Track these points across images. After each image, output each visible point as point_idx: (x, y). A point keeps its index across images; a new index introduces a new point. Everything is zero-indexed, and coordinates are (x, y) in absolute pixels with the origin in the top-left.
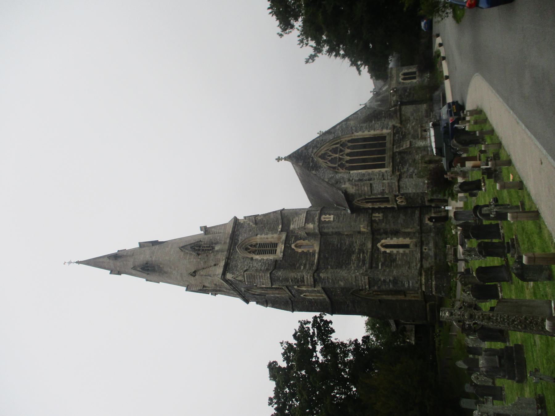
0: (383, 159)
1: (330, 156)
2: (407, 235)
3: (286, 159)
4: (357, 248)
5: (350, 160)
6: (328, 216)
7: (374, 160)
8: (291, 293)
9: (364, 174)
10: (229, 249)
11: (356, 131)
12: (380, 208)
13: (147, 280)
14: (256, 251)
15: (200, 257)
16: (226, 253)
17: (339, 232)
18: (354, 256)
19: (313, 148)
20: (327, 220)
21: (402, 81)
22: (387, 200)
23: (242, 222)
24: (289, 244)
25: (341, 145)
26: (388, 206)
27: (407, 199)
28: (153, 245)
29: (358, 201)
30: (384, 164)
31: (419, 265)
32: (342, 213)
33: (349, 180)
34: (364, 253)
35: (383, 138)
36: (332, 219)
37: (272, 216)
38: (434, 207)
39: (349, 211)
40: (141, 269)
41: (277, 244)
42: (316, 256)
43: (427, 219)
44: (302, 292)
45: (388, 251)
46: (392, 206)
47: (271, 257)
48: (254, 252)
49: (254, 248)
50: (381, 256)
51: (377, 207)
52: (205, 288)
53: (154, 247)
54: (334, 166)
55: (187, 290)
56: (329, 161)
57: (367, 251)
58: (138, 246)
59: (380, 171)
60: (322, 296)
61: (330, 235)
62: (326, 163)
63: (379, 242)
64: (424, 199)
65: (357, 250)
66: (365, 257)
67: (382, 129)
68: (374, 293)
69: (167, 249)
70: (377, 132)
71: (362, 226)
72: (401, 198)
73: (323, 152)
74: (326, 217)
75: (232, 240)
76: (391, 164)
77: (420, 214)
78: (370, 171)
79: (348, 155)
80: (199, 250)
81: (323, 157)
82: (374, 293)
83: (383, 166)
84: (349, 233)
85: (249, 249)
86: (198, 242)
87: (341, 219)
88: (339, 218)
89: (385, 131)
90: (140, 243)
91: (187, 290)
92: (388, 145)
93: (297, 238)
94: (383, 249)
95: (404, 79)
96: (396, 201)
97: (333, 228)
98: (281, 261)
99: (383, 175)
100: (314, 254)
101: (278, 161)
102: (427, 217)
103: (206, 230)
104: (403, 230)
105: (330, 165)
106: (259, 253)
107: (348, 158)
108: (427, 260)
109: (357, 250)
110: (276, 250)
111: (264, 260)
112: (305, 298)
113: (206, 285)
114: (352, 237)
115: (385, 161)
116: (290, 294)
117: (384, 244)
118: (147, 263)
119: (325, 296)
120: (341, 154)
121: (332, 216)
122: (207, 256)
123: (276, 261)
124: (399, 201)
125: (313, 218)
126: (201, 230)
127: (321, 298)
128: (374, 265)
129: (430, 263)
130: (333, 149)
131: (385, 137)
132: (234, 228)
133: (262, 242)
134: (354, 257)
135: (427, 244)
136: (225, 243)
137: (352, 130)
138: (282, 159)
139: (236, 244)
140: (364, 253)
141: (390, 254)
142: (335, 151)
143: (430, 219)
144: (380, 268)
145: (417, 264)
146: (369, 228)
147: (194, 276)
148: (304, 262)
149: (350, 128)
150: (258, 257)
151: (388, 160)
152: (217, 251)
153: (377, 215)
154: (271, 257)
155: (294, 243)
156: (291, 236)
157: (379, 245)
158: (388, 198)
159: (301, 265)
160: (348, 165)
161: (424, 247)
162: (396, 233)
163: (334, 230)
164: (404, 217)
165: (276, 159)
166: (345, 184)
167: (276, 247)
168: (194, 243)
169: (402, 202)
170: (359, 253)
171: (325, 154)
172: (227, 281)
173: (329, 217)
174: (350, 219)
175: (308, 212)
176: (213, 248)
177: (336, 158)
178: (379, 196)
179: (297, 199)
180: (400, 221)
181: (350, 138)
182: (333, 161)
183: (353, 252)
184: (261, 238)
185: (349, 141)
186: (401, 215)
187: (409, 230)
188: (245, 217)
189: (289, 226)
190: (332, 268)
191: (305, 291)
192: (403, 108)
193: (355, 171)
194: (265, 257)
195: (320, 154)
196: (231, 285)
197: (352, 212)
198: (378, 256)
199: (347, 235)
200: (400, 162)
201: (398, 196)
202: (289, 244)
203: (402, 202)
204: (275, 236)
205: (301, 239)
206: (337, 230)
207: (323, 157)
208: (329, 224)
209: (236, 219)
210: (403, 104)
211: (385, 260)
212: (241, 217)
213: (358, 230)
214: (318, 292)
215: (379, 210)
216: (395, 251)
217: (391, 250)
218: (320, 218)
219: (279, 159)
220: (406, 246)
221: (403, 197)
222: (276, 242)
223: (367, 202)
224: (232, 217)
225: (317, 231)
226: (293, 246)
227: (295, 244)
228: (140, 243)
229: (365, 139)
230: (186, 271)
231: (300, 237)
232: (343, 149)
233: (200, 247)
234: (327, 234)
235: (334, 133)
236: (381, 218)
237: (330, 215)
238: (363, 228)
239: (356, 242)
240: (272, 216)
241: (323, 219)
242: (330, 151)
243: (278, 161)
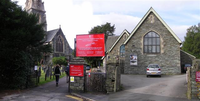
0: (58, 51)
3: (60, 27)
7: (58, 49)
35: (62, 52)
81: (60, 37)
83: (56, 51)
89: (64, 52)
92: (61, 52)
103: (43, 3)
142: (61, 40)
151: (57, 52)
160: (57, 43)
179: (49, 28)
207: (60, 37)
209: (46, 12)
210: (70, 56)
212: (46, 13)
219: (60, 25)
229: (63, 47)
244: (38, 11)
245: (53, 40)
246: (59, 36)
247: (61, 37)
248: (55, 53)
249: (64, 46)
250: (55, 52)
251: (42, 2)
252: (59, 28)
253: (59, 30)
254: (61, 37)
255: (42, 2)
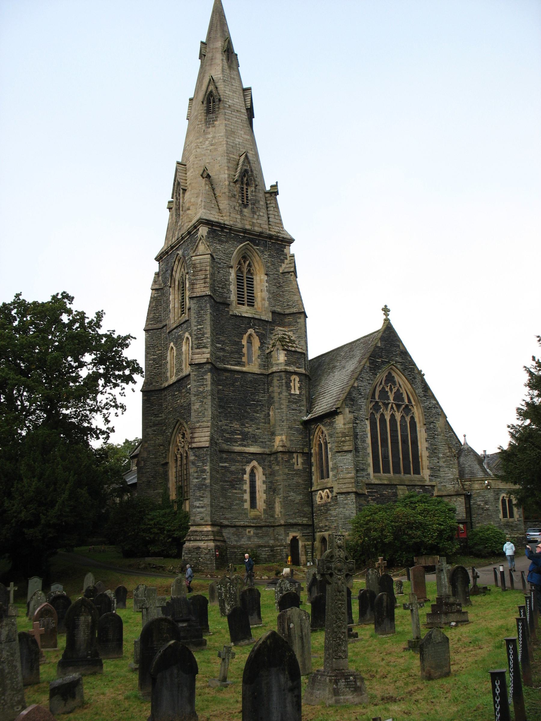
0: (386, 470)
1: (391, 390)
2: (270, 504)
3: (387, 321)
4: (250, 429)
5: (385, 420)
6: (297, 385)
8: (176, 327)
9: (364, 442)
10: (245, 231)
11: (427, 430)
12: (311, 465)
13: (191, 100)
14: (242, 273)
15: (232, 184)
16: (239, 225)
17: (274, 402)
18: (238, 426)
19: (402, 364)
20: (292, 384)
21: (501, 498)
22: (324, 474)
23: (286, 251)
24: (254, 325)
25: (407, 406)
26: (314, 477)
27: (325, 505)
28: (247, 109)
29: (322, 433)
30: (379, 472)
31: (226, 522)
32: (303, 408)
33: (356, 418)
34: (243, 440)
35: (417, 471)
36: (293, 392)
37: (296, 298)
38: (313, 544)
39: (305, 418)
40: (211, 92)
41: (253, 306)
42: (237, 368)
43: (295, 534)
44: (179, 346)
45: (246, 477)
46: (315, 484)
47: (233, 297)
48: (240, 270)
49: (245, 271)
50: (238, 466)
51: (313, 460)
52: (181, 191)
53: (245, 112)
54: (377, 397)
55: (178, 163)
56: (383, 388)
57: (245, 446)
58: (245, 86)
59: (369, 465)
60: (171, 377)
61: (268, 389)
62: (381, 383)
63: (259, 464)
64: (326, 531)
65: (246, 429)
66: (236, 442)
67: (431, 469)
68: (179, 456)
69: (242, 132)
70: (425, 462)
71: (284, 437)
72: (328, 497)
73: (397, 378)
74: (297, 382)
75: (259, 236)
76: (377, 482)
77: (302, 525)
78: (370, 450)
79: (393, 416)
80: (242, 183)
82: (179, 456)
83: (376, 470)
84: (271, 417)
85: (245, 262)
86: (255, 181)
87: (294, 406)
88: (296, 403)
89: (426, 473)
90: (250, 89)
91: (178, 163)
93: (262, 338)
94: (248, 469)
95: (503, 501)
96: (323, 490)
97: (280, 393)
98: (228, 312)
99: (363, 470)
100: (240, 364)
101: (383, 310)
102: (298, 534)
103: (274, 192)
104: (277, 500)
105: (378, 389)
106: (239, 279)
107: (388, 418)
108: (234, 534)
109: (246, 429)
110: (243, 304)
111: (229, 285)
112: (167, 349)
113: (187, 194)
114: (265, 423)
115: (383, 473)
116: (175, 326)
117: (255, 471)
118: (220, 100)
119: (174, 379)
120: (394, 406)
121: (298, 392)
122: (234, 196)
123: (228, 305)
124: (324, 494)
125: (294, 363)
126: (271, 186)
127: (169, 374)
128: (224, 456)
129: (229, 538)
130: (402, 394)
131: (419, 474)
132: (277, 238)
133: (255, 283)
134: (236, 425)
135: (256, 535)
136: (253, 224)
137: (430, 423)
138: (387, 315)
139: (252, 240)
140: (243, 440)
141: (242, 480)
142: (398, 396)
143: (295, 540)
144: (221, 464)
145: (228, 519)
146: (281, 449)
147: (202, 175)
148: (227, 348)
149: (432, 420)
150: (233, 275)
152: (241, 212)
153: (300, 460)
154: (233, 297)
155: (255, 332)
156: (264, 328)
157: (254, 463)
158: (328, 477)
159: (223, 343)
160: (378, 416)
161: (253, 531)
162: (271, 489)
163: (276, 395)
164: (297, 501)
165: (386, 306)
166: (350, 412)
167: (248, 305)
168: (252, 175)
169: (321, 498)
170: (242, 433)
171: (394, 383)
172: (195, 227)
173: (297, 388)
174: (295, 420)
175: (304, 355)
176: (246, 206)
177: (388, 398)
178: (330, 464)
180: (293, 495)
181: (417, 420)
182: (384, 394)
183: (243, 424)
184: (261, 280)
185: (412, 418)
186: (300, 497)
187: (278, 508)
188: (293, 256)
189: (279, 325)
190: (219, 391)
191: (179, 349)
192: (461, 499)
193: (369, 428)
194: (233, 288)
195: (394, 374)
196: (189, 233)
197: (306, 423)
198: (238, 462)
199: (269, 415)
200: (382, 495)
201: (331, 492)
202: (254, 325)
203: (321, 498)
204: (267, 304)
205: (262, 343)
206: (276, 399)
207: (390, 379)
208: (284, 388)
210: (468, 498)
211: (232, 473)
212: (293, 249)
213: (277, 432)
214: (179, 370)
215: (308, 463)
216: (247, 487)
217: (248, 482)
218: (295, 373)
219: (386, 310)
220: (253, 504)
221: (329, 500)
222: (255, 303)
223: (320, 445)
224: (294, 237)
225: (275, 369)
226: (250, 331)
227: (254, 335)
228: (250, 89)
230: (209, 163)
231: (264, 343)
232: (401, 409)
233: (247, 184)
234: (270, 384)
235: (425, 396)
236: (296, 467)
237: (300, 388)
238: (279, 441)
239: (258, 429)
240: (296, 298)
241: (293, 377)
242: (398, 390)
243: (383, 310)
244: (244, 239)
245: (350, 398)
246: (382, 375)
247: (400, 379)
248: (369, 485)
249: (422, 434)
250: (373, 479)
251: (268, 188)
252: (377, 325)
253: (382, 339)
254: (400, 379)
255: (268, 188)
